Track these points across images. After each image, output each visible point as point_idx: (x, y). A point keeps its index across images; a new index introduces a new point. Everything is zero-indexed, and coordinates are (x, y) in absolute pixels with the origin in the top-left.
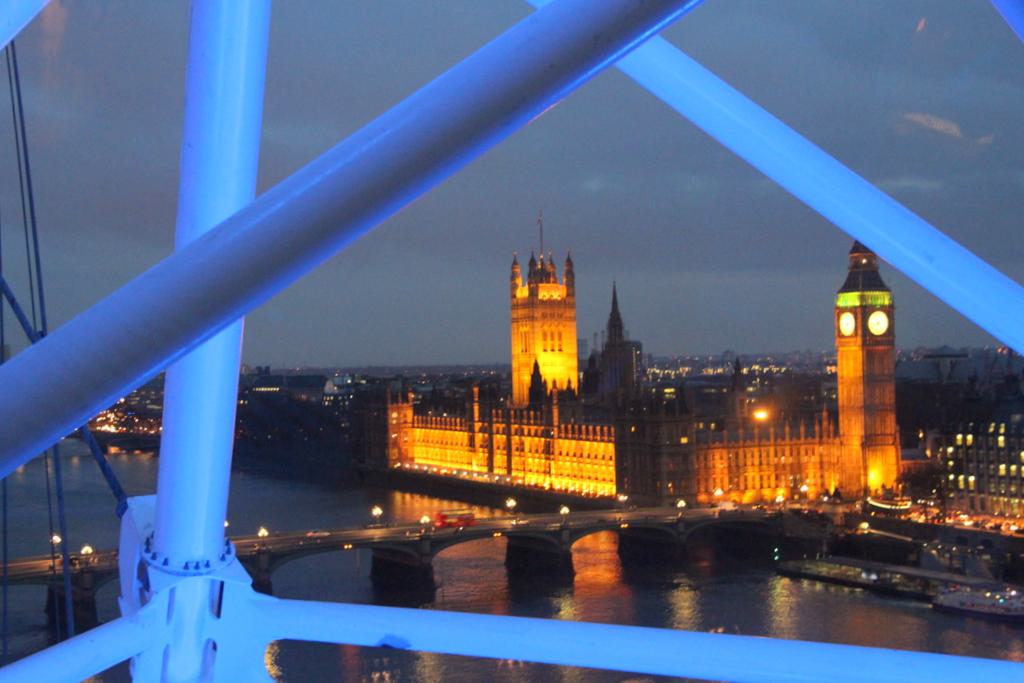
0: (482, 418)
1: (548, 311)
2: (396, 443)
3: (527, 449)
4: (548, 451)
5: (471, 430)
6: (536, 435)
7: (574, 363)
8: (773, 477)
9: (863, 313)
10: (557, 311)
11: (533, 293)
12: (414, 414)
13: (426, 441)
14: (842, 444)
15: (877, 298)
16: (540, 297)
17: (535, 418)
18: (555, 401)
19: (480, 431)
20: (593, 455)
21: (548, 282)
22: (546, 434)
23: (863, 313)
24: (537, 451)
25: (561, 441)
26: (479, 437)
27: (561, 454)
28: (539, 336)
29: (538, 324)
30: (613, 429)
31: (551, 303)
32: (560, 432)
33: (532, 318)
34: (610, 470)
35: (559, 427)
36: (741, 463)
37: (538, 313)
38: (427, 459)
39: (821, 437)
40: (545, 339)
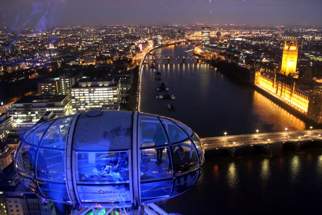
0: (276, 81)
1: (292, 52)
2: (256, 80)
4: (291, 95)
6: (288, 90)
7: (296, 64)
10: (294, 52)
11: (289, 48)
12: (261, 74)
16: (290, 49)
17: (289, 87)
18: (294, 86)
19: (275, 84)
21: (292, 46)
22: (291, 92)
24: (288, 94)
25: (294, 94)
26: (275, 85)
28: (289, 58)
29: (289, 55)
30: (308, 97)
31: (292, 51)
32: (294, 92)
33: (288, 54)
34: (307, 106)
35: (294, 91)
37: (289, 53)
40: (290, 58)
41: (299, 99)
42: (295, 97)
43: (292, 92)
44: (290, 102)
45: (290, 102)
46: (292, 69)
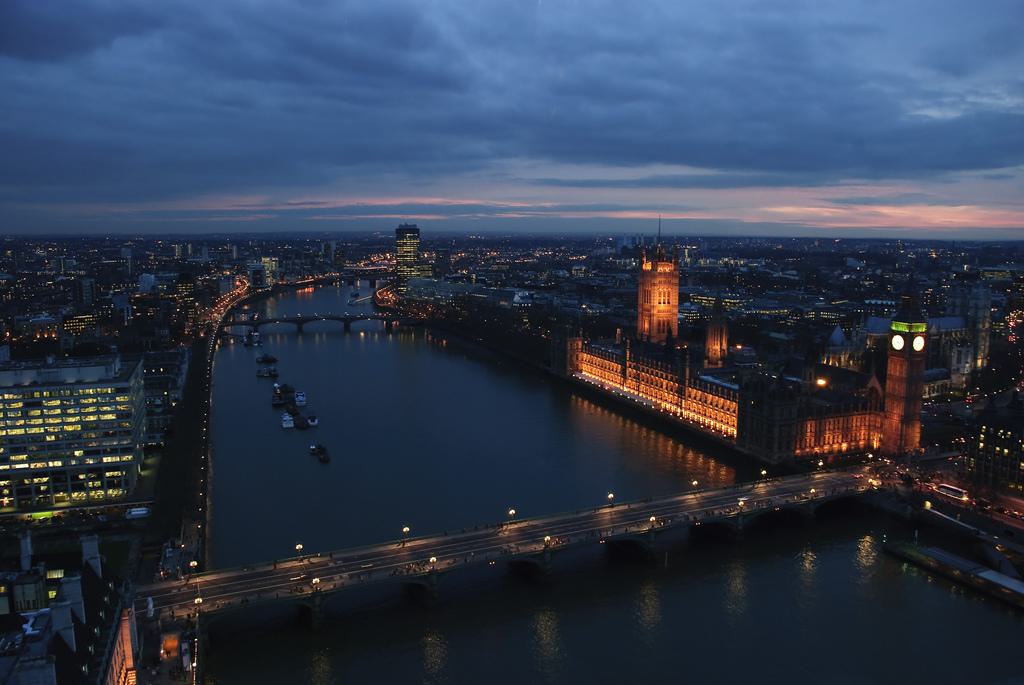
3: (664, 387)
4: (681, 393)
5: (624, 364)
8: (840, 437)
9: (909, 338)
13: (591, 363)
14: (886, 417)
15: (918, 327)
20: (714, 404)
22: (681, 382)
23: (909, 338)
27: (690, 396)
35: (689, 380)
36: (822, 429)
38: (591, 373)
39: (870, 409)
41: (706, 402)
42: (693, 396)
43: (684, 384)
44: (678, 414)
45: (678, 414)
46: (668, 324)
